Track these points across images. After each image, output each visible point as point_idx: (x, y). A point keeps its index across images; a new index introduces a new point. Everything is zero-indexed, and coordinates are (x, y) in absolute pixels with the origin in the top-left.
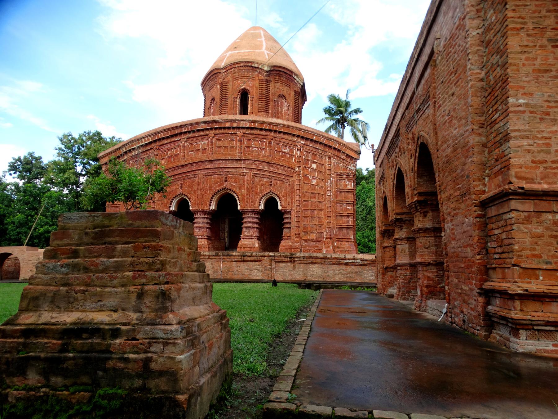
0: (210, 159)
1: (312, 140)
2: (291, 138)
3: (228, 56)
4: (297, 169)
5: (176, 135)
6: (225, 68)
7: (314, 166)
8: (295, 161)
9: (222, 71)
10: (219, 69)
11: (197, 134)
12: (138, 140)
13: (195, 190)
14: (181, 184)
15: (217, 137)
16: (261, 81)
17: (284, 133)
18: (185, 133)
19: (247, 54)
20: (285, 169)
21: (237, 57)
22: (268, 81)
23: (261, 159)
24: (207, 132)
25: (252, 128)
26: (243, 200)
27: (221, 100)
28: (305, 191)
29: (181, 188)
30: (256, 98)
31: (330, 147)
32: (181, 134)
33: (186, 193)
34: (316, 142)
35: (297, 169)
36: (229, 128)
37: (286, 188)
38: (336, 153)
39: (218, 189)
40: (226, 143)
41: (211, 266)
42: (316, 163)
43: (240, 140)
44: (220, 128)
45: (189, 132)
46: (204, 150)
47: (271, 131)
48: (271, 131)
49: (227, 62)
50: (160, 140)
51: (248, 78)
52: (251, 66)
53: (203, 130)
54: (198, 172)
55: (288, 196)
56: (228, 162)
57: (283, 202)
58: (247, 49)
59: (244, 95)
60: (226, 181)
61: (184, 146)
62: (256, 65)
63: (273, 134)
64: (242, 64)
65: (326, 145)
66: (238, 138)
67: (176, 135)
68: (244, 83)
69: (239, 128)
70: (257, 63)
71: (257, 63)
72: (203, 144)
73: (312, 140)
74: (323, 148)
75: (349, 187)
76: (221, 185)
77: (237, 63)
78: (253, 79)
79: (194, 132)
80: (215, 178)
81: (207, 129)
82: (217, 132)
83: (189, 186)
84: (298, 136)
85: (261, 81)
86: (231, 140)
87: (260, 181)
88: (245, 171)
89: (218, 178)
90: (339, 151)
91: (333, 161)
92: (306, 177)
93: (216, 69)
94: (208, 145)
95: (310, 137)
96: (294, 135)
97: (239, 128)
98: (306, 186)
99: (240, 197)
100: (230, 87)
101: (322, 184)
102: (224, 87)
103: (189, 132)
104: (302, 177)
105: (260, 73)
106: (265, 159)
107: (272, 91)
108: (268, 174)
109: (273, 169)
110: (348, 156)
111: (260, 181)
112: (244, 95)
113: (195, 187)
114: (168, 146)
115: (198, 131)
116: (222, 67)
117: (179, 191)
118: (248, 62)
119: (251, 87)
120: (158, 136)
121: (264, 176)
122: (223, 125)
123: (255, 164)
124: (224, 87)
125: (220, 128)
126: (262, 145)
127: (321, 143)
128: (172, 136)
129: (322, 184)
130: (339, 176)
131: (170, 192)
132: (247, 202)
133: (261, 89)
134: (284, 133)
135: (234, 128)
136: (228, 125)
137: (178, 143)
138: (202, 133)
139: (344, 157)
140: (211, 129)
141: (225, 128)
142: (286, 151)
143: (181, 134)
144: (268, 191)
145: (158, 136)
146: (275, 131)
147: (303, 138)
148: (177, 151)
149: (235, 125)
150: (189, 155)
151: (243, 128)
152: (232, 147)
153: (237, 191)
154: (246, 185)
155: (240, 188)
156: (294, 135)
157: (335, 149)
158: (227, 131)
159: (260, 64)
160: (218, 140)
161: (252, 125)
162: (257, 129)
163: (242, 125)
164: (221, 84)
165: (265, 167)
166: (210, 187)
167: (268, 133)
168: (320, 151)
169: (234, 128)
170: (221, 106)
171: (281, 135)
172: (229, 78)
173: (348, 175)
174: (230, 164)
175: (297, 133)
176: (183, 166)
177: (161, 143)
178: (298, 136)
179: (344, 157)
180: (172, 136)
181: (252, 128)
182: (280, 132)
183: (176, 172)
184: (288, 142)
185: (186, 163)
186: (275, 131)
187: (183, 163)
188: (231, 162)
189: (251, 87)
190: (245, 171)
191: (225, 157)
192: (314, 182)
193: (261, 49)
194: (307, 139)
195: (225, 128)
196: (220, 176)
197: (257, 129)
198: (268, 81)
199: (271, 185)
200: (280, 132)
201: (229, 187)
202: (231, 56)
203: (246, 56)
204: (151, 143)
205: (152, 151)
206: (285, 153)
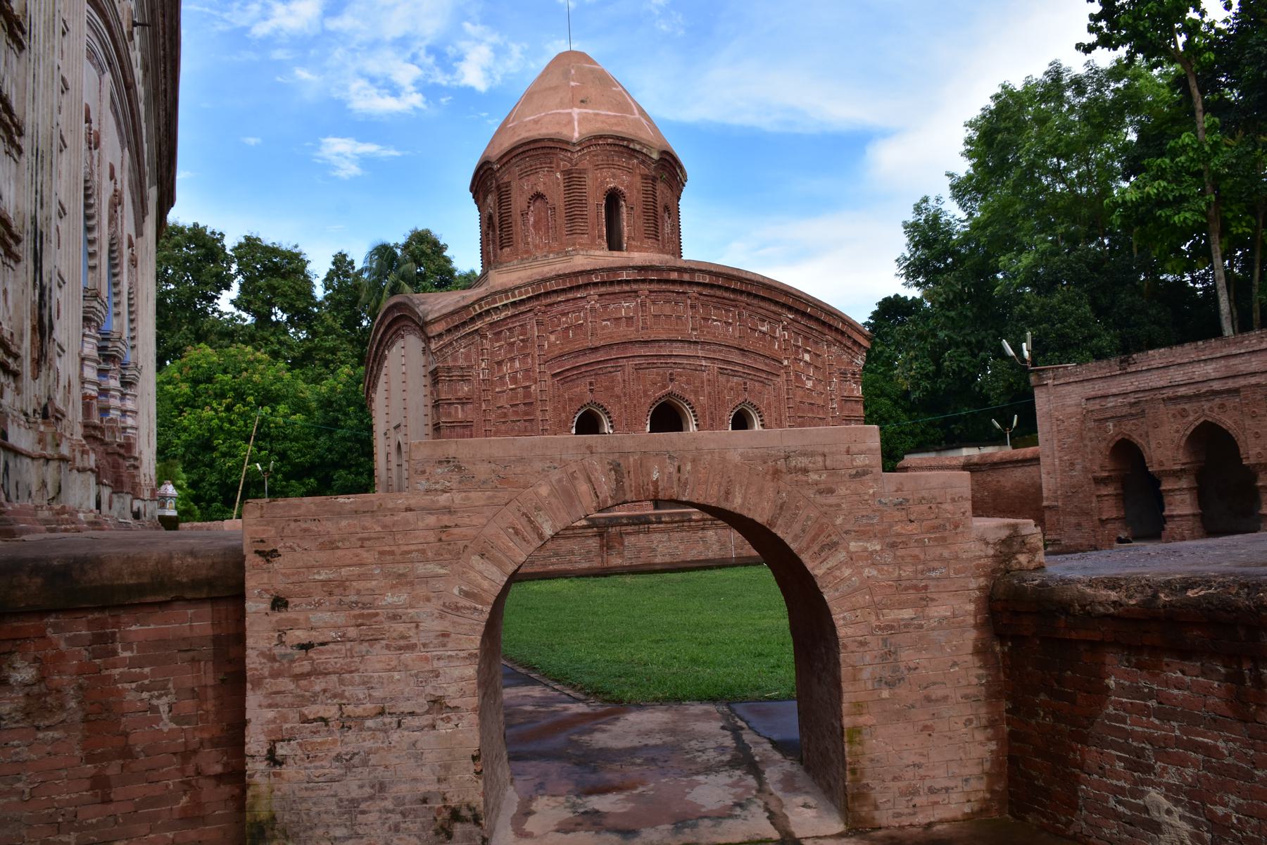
0: (646, 338)
1: (804, 314)
2: (773, 308)
3: (576, 117)
4: (786, 363)
5: (579, 287)
6: (580, 143)
7: (807, 357)
8: (780, 347)
9: (569, 148)
10: (567, 143)
11: (617, 289)
12: (505, 291)
13: (618, 397)
14: (591, 384)
15: (653, 296)
16: (645, 177)
17: (763, 299)
18: (596, 284)
19: (613, 121)
20: (767, 361)
21: (599, 125)
22: (654, 179)
23: (730, 343)
24: (635, 287)
25: (711, 286)
26: (704, 416)
27: (569, 205)
28: (798, 399)
29: (591, 391)
30: (638, 210)
31: (830, 327)
32: (586, 286)
33: (602, 402)
34: (810, 317)
35: (786, 363)
36: (674, 282)
37: (768, 395)
38: (839, 337)
39: (658, 394)
40: (667, 309)
41: (715, 538)
42: (809, 352)
43: (692, 307)
44: (659, 281)
45: (603, 283)
46: (629, 319)
47: (742, 292)
48: (742, 292)
49: (584, 132)
50: (547, 294)
51: (620, 168)
52: (627, 147)
53: (627, 282)
54: (622, 362)
55: (773, 409)
56: (675, 345)
57: (767, 421)
58: (609, 110)
59: (613, 199)
60: (672, 380)
61: (593, 310)
62: (638, 147)
63: (744, 298)
64: (610, 141)
65: (824, 323)
66: (689, 302)
67: (579, 287)
68: (614, 176)
69: (690, 283)
70: (640, 143)
71: (640, 143)
72: (626, 307)
73: (804, 314)
74: (819, 328)
75: (856, 393)
76: (664, 387)
77: (601, 137)
78: (630, 172)
79: (612, 283)
80: (652, 374)
81: (636, 281)
82: (654, 287)
83: (607, 389)
84: (783, 305)
85: (645, 177)
86: (676, 303)
87: (728, 381)
88: (704, 363)
89: (658, 374)
90: (843, 333)
91: (834, 349)
92: (798, 376)
93: (551, 140)
94: (636, 311)
95: (802, 308)
96: (777, 303)
97: (690, 283)
98: (800, 392)
99: (698, 410)
100: (589, 182)
101: (820, 388)
102: (573, 179)
103: (603, 283)
104: (793, 378)
105: (643, 162)
106: (735, 343)
107: (659, 199)
108: (741, 369)
109: (748, 362)
110: (855, 342)
111: (728, 381)
112: (613, 199)
113: (617, 390)
114: (562, 307)
115: (620, 282)
116: (574, 141)
117: (589, 397)
118: (623, 139)
119: (627, 187)
120: (545, 287)
121: (735, 374)
122: (665, 276)
123: (720, 351)
124: (573, 179)
125: (659, 281)
126: (727, 317)
127: (817, 320)
128: (571, 289)
129: (820, 388)
130: (844, 374)
131: (571, 399)
132: (712, 419)
133: (645, 192)
134: (763, 299)
135: (682, 283)
136: (674, 276)
137: (583, 303)
138: (627, 288)
139: (849, 344)
140: (643, 281)
141: (667, 281)
142: (764, 329)
143: (586, 286)
144: (741, 399)
145: (545, 287)
146: (749, 294)
147: (790, 309)
148: (578, 318)
149: (686, 277)
150: (604, 328)
151: (698, 284)
152: (679, 318)
153: (692, 398)
154: (707, 389)
155: (696, 393)
156: (777, 303)
157: (837, 330)
158: (671, 288)
159: (644, 146)
160: (654, 302)
161: (714, 280)
162: (720, 287)
163: (698, 278)
164: (567, 173)
165: (735, 357)
166: (645, 392)
167: (739, 297)
168: (816, 334)
169: (682, 283)
170: (571, 218)
171: (755, 302)
172: (586, 163)
173: (854, 374)
174: (678, 350)
175: (783, 300)
176: (596, 349)
177: (549, 301)
178: (783, 305)
179: (849, 344)
180: (571, 289)
181: (711, 286)
182: (756, 296)
183: (582, 360)
184: (768, 314)
185: (602, 343)
186: (749, 294)
187: (597, 344)
188: (679, 345)
189: (627, 187)
190: (704, 363)
191: (673, 336)
192: (809, 384)
193: (633, 114)
194: (797, 311)
195: (667, 281)
196: (661, 371)
197: (720, 287)
198: (654, 179)
199: (745, 389)
200: (756, 296)
201: (678, 392)
202: (583, 119)
203: (618, 124)
204: (529, 298)
205: (530, 314)
206: (764, 333)
